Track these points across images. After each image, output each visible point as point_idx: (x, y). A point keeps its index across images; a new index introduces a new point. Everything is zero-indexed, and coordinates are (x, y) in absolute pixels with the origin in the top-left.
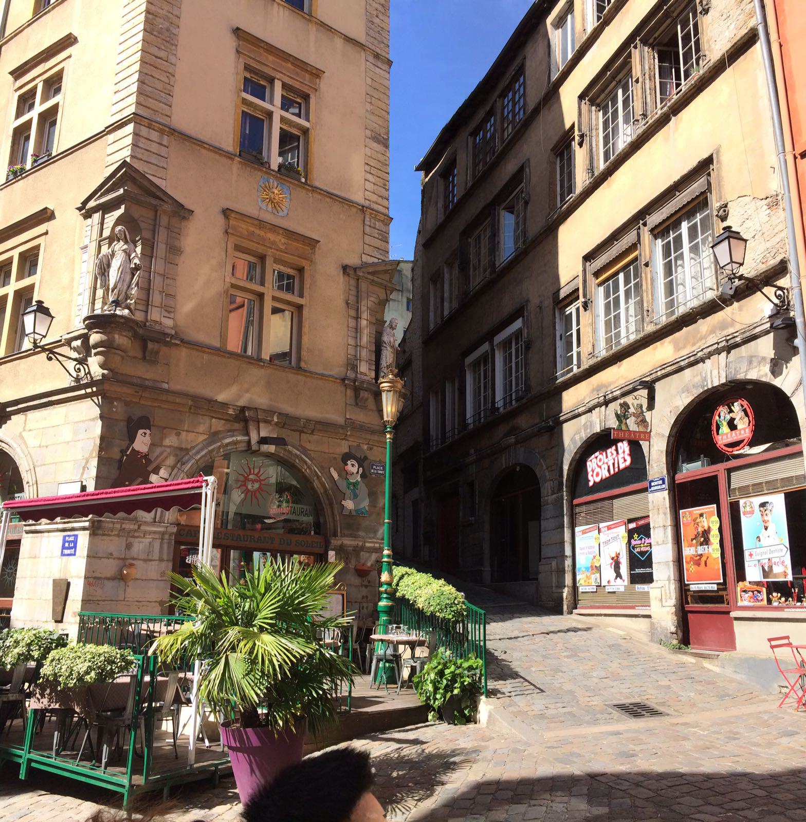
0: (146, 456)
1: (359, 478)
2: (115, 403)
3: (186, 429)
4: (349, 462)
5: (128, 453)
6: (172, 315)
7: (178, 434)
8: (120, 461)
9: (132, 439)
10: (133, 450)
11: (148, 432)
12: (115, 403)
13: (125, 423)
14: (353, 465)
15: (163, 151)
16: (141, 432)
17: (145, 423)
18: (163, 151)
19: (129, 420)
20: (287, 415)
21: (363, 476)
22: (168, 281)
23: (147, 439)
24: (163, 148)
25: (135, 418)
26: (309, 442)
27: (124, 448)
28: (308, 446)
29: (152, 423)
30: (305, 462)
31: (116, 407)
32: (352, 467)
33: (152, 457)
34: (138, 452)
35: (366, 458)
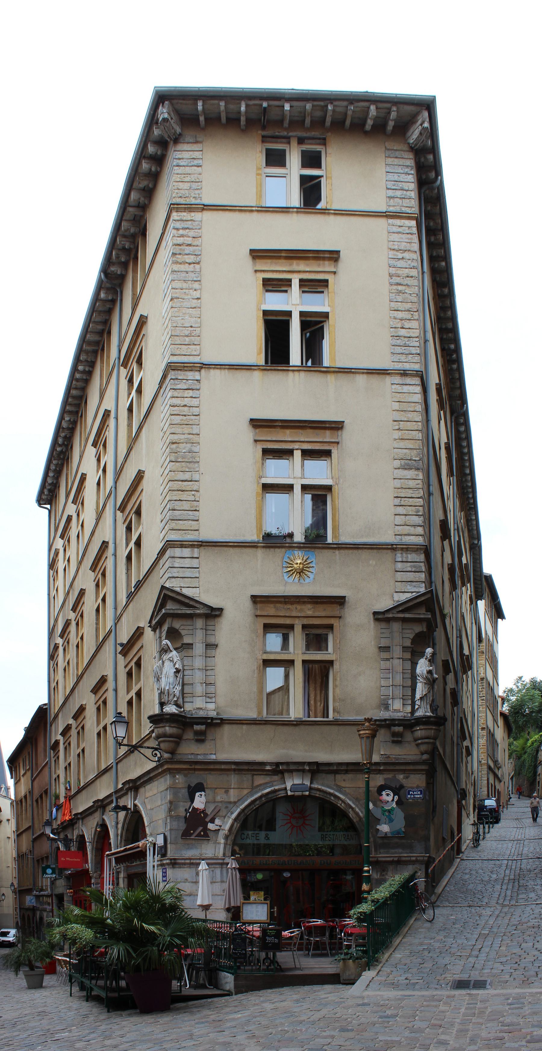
0: (203, 811)
8: (185, 817)
9: (192, 800)
10: (194, 808)
11: (203, 793)
13: (186, 790)
16: (198, 794)
17: (200, 787)
19: (189, 787)
22: (209, 673)
25: (193, 785)
28: (343, 784)
31: (178, 779)
33: (209, 812)
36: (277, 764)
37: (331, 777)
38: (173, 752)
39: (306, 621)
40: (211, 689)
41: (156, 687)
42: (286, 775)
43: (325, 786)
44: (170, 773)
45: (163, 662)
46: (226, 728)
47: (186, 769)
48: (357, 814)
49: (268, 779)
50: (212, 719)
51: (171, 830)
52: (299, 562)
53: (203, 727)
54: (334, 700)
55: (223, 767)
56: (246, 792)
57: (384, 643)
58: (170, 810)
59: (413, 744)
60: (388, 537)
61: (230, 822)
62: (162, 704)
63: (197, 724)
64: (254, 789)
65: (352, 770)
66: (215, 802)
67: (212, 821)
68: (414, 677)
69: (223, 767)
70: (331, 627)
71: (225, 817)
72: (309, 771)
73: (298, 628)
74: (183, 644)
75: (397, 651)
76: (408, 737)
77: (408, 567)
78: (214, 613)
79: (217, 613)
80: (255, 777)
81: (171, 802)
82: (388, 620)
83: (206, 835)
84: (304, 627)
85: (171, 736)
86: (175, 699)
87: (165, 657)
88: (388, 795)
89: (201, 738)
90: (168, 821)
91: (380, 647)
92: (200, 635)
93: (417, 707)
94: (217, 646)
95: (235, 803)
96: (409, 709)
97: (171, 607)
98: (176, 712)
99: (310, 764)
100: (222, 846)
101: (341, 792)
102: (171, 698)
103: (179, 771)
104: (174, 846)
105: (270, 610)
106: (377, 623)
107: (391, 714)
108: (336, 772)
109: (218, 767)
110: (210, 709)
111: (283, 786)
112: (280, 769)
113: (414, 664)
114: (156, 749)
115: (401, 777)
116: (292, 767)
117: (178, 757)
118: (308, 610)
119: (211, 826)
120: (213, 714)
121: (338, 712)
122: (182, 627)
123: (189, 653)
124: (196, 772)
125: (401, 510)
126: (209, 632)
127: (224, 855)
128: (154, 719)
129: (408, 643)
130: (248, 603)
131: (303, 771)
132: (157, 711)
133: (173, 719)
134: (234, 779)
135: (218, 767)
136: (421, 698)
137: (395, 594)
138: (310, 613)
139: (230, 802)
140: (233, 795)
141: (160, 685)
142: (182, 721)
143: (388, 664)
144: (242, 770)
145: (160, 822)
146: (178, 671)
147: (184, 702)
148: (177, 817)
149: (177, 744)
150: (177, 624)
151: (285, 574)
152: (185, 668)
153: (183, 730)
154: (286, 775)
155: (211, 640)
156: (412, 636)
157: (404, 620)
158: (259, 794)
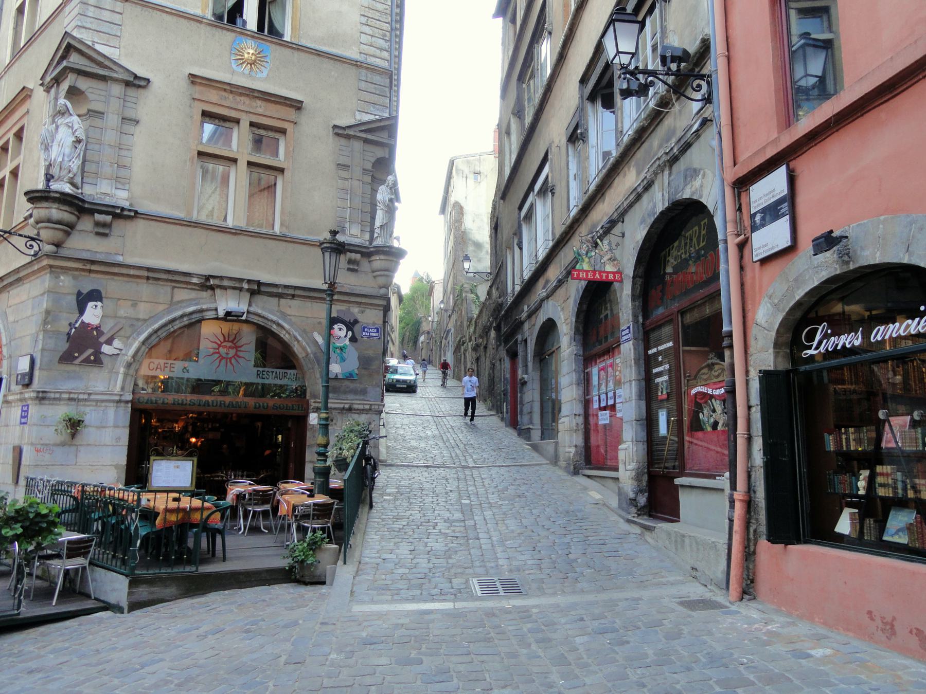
0: (97, 328)
1: (347, 342)
2: (62, 278)
3: (144, 299)
4: (336, 327)
5: (77, 325)
6: (127, 187)
7: (134, 305)
8: (68, 334)
9: (82, 311)
10: (83, 322)
11: (99, 304)
12: (62, 278)
13: (75, 297)
14: (340, 329)
15: (117, 18)
16: (91, 304)
17: (95, 295)
18: (117, 18)
19: (79, 293)
20: (259, 283)
21: (353, 339)
22: (123, 153)
23: (99, 312)
24: (116, 15)
25: (85, 292)
26: (290, 307)
27: (73, 322)
28: (289, 311)
29: (103, 295)
30: (282, 327)
31: (62, 281)
32: (340, 331)
33: (105, 329)
34: (88, 324)
35: (356, 322)
36: (208, 278)
37: (274, 301)
38: (58, 245)
39: (255, 119)
40: (123, 173)
41: (42, 157)
42: (218, 291)
43: (266, 309)
44: (51, 272)
45: (57, 127)
46: (140, 224)
47: (77, 269)
48: (304, 349)
49: (194, 294)
50: (123, 209)
51: (43, 350)
52: (251, 51)
53: (108, 218)
54: (282, 213)
55: (132, 272)
56: (161, 308)
57: (343, 160)
58: (45, 322)
59: (370, 275)
60: (352, 53)
61: (136, 345)
62: (49, 178)
63: (101, 212)
64: (172, 304)
65: (299, 296)
66: (115, 317)
67: (109, 342)
68: (374, 205)
69: (132, 272)
70: (283, 132)
71: (128, 338)
72: (248, 290)
73: (245, 124)
74: (89, 110)
75: (357, 172)
76: (365, 265)
77: (371, 88)
78: (137, 82)
79: (143, 83)
80: (176, 290)
81: (48, 312)
82: (348, 137)
83: (97, 360)
84: (252, 124)
85: (59, 222)
86: (71, 175)
87: (60, 121)
88: (340, 329)
89: (103, 231)
90: (41, 337)
91: (339, 164)
92: (115, 104)
93: (376, 235)
94: (138, 122)
95: (145, 320)
96: (367, 236)
97: (75, 59)
98: (70, 192)
99: (249, 281)
100: (121, 377)
101: (285, 320)
102: (64, 173)
103: (65, 270)
104: (45, 373)
105: (213, 96)
106: (337, 138)
107: (348, 238)
108: (280, 296)
109: (124, 271)
110: (121, 198)
111: (213, 306)
112: (208, 284)
113: (374, 191)
114: (33, 239)
115: (355, 310)
116: (226, 283)
117: (64, 252)
118: (260, 107)
119: (106, 349)
120: (126, 204)
121: (287, 227)
122: (90, 90)
123: (98, 122)
124: (93, 275)
125: (367, 29)
126: (128, 104)
127: (123, 389)
129: (369, 166)
130: (184, 83)
131: (241, 289)
132: (41, 186)
133: (65, 199)
134: (145, 290)
135: (124, 271)
136: (381, 227)
137: (357, 113)
138: (260, 111)
139: (138, 320)
140: (143, 310)
141: (49, 155)
142: (78, 205)
143: (347, 184)
144: (159, 279)
145: (28, 339)
146: (79, 141)
147: (82, 183)
148: (57, 333)
149: (68, 234)
150: (83, 84)
151: (233, 62)
152: (90, 140)
153: (79, 218)
154: (218, 291)
155: (130, 114)
156: (373, 160)
157: (366, 141)
158: (180, 313)
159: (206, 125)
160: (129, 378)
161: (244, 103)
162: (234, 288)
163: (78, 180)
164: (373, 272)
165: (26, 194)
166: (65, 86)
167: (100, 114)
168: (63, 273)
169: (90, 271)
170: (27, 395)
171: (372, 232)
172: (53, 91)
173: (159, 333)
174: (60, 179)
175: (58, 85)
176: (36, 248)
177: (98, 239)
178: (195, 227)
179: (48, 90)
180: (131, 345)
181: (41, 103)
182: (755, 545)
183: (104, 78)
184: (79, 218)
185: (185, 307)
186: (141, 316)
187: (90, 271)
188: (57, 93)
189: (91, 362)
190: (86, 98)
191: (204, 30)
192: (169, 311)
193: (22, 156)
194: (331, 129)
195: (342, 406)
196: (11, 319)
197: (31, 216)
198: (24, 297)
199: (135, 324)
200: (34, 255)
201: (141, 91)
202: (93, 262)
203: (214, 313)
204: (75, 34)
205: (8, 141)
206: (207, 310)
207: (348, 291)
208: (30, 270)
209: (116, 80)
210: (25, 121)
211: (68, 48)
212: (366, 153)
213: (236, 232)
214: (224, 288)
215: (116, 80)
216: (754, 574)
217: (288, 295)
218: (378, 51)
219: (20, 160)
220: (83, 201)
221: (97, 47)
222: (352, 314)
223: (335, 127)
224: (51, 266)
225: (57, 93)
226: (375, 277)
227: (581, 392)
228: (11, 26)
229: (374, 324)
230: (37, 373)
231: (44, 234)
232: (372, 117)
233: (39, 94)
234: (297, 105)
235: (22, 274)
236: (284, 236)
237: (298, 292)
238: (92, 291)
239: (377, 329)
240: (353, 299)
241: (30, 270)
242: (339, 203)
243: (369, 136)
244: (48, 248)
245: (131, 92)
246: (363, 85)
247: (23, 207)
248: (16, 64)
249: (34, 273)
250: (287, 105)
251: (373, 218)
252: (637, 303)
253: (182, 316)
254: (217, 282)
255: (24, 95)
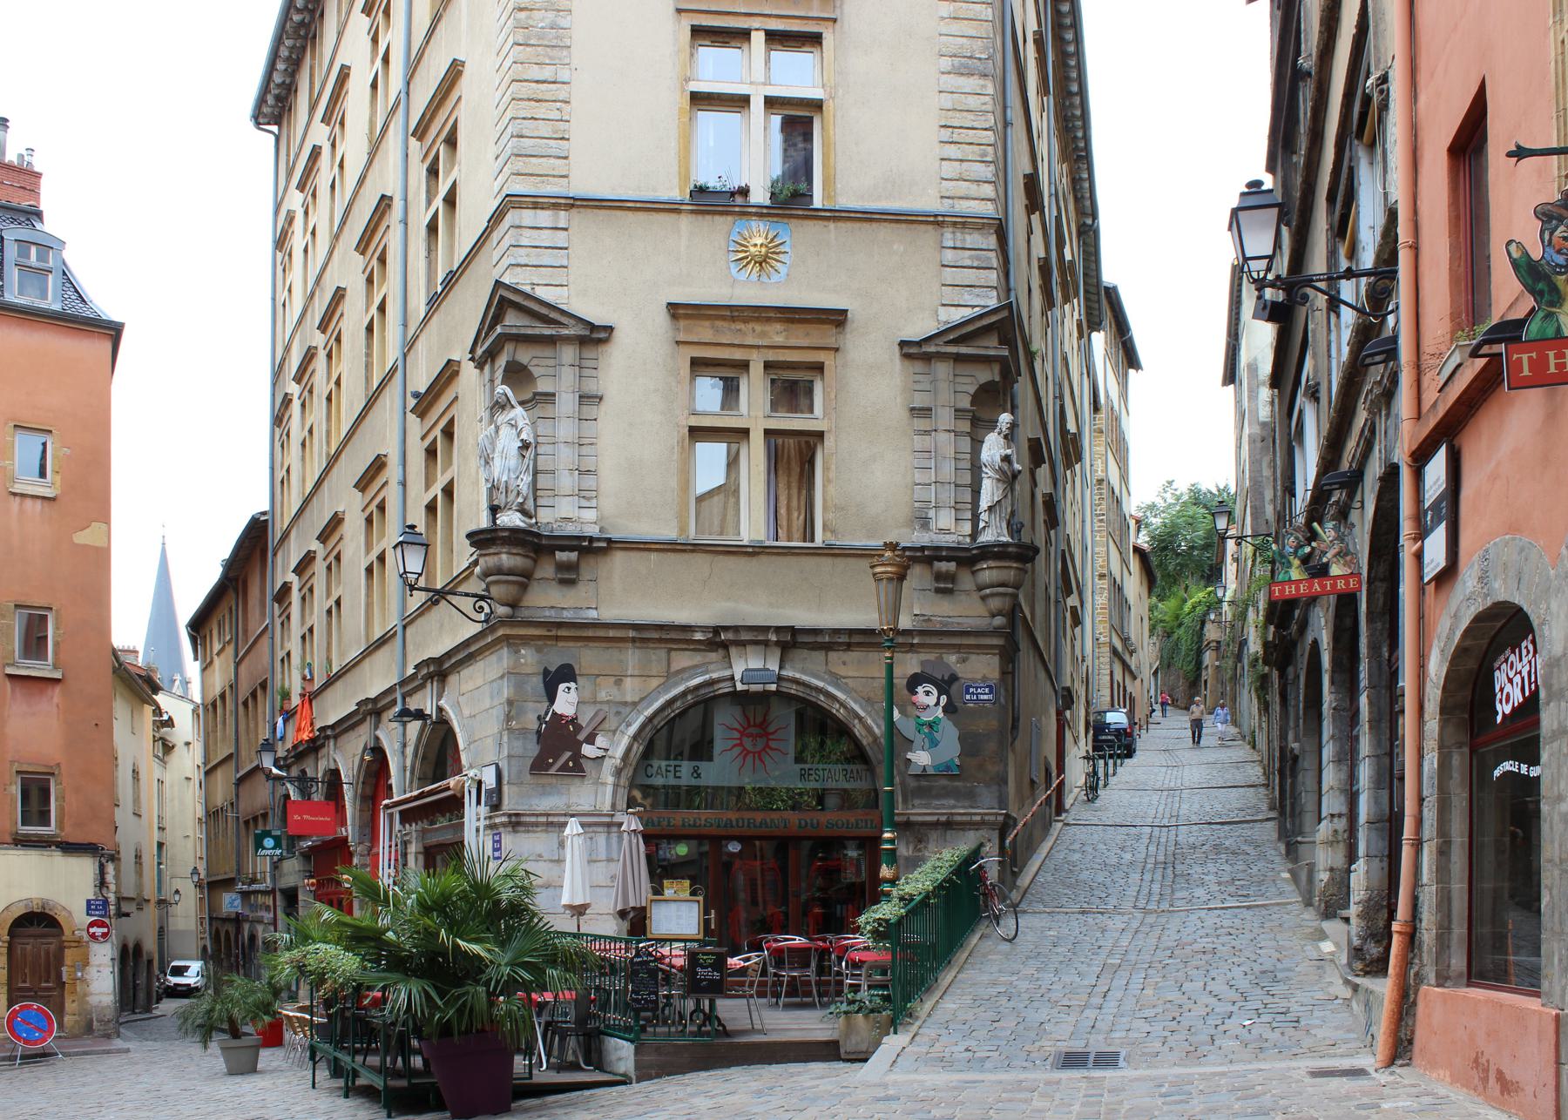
0: (573, 721)
1: (940, 713)
8: (538, 732)
9: (552, 698)
10: (554, 714)
11: (572, 685)
13: (541, 678)
15: (560, 239)
16: (562, 686)
17: (566, 673)
19: (546, 672)
21: (949, 709)
22: (585, 450)
25: (553, 669)
28: (842, 671)
31: (524, 657)
33: (583, 721)
35: (954, 678)
36: (717, 630)
37: (819, 656)
38: (514, 605)
39: (772, 356)
40: (589, 482)
41: (483, 476)
42: (733, 651)
43: (807, 672)
44: (509, 645)
45: (497, 429)
46: (619, 558)
47: (540, 637)
48: (869, 729)
49: (697, 658)
50: (591, 539)
51: (509, 756)
52: (759, 241)
53: (574, 556)
54: (825, 508)
55: (611, 633)
56: (655, 682)
57: (920, 401)
58: (508, 718)
59: (976, 596)
60: (928, 202)
61: (625, 741)
62: (494, 510)
63: (563, 549)
64: (670, 676)
65: (859, 644)
66: (595, 702)
67: (590, 740)
68: (976, 468)
69: (611, 633)
70: (819, 368)
71: (614, 732)
72: (777, 643)
73: (757, 369)
74: (535, 394)
75: (945, 418)
76: (966, 581)
77: (965, 258)
78: (595, 335)
79: (603, 335)
80: (673, 654)
81: (510, 703)
82: (928, 358)
83: (576, 768)
84: (768, 366)
85: (510, 572)
86: (520, 500)
87: (502, 418)
88: (928, 693)
89: (568, 577)
90: (505, 739)
91: (913, 409)
92: (568, 376)
93: (982, 525)
94: (601, 399)
95: (635, 704)
96: (967, 528)
97: (512, 321)
98: (522, 525)
99: (778, 629)
100: (609, 789)
101: (837, 686)
102: (511, 497)
103: (526, 640)
104: (515, 788)
105: (704, 332)
106: (907, 363)
107: (934, 537)
108: (827, 647)
109: (601, 633)
110: (587, 522)
111: (727, 673)
112: (720, 640)
113: (977, 443)
114: (482, 598)
115: (952, 659)
116: (744, 636)
117: (524, 614)
118: (777, 334)
119: (587, 750)
120: (593, 531)
121: (833, 532)
122: (535, 362)
123: (548, 410)
124: (561, 644)
125: (952, 151)
126: (586, 372)
127: (613, 806)
128: (482, 540)
129: (965, 403)
130: (662, 317)
131: (766, 643)
132: (484, 522)
133: (516, 538)
134: (632, 658)
135: (601, 633)
136: (990, 508)
137: (941, 309)
138: (779, 340)
139: (625, 704)
140: (631, 689)
141: (491, 473)
142: (533, 543)
143: (927, 442)
144: (648, 640)
145: (489, 741)
146: (525, 446)
147: (536, 506)
148: (523, 732)
149: (524, 587)
150: (524, 355)
151: (732, 265)
152: (540, 440)
153: (535, 561)
154: (733, 651)
155: (591, 387)
156: (972, 390)
157: (958, 359)
158: (681, 688)
159: (699, 380)
160: (621, 790)
161: (751, 334)
162: (756, 643)
163: (530, 505)
164: (980, 589)
165: (469, 536)
166: (502, 361)
167: (549, 397)
168: (525, 645)
169: (557, 638)
170: (497, 820)
171: (975, 518)
172: (487, 368)
173: (655, 722)
174: (507, 507)
175: (493, 361)
176: (487, 610)
177: (565, 589)
178: (692, 551)
179: (480, 366)
180: (618, 744)
181: (470, 378)
182: (1416, 994)
183: (551, 341)
184: (535, 561)
185: (688, 679)
186: (629, 699)
187: (557, 638)
188: (493, 372)
189: (571, 770)
190: (530, 374)
191: (685, 222)
192: (664, 687)
193: (455, 466)
194: (897, 348)
195: (935, 818)
196: (466, 712)
197: (476, 563)
198: (480, 682)
199: (626, 707)
200: (486, 621)
201: (601, 348)
202: (560, 625)
203: (728, 684)
204: (506, 280)
205: (435, 439)
206: (719, 680)
207: (938, 627)
208: (482, 643)
209: (567, 340)
210: (453, 411)
211: (503, 301)
212: (959, 379)
213: (756, 551)
214: (742, 644)
215: (567, 340)
216: (1413, 1032)
217: (840, 644)
218: (974, 186)
219: (453, 471)
220: (538, 535)
221: (541, 293)
222: (947, 665)
223: (903, 344)
224: (507, 637)
225: (493, 372)
226: (983, 598)
227: (1343, 776)
228: (423, 253)
229: (984, 679)
230: (505, 789)
231: (495, 591)
232: (967, 313)
233: (469, 371)
234: (836, 318)
235: (473, 649)
236: (830, 547)
237: (856, 639)
238: (563, 667)
239: (990, 687)
240: (946, 641)
241: (482, 643)
242: (919, 477)
243: (963, 350)
244: (502, 610)
245: (589, 353)
246: (949, 256)
247: (464, 554)
248: (435, 318)
249: (488, 647)
250: (822, 322)
251: (976, 493)
252: (1379, 625)
253: (684, 694)
254: (729, 636)
255: (449, 373)
